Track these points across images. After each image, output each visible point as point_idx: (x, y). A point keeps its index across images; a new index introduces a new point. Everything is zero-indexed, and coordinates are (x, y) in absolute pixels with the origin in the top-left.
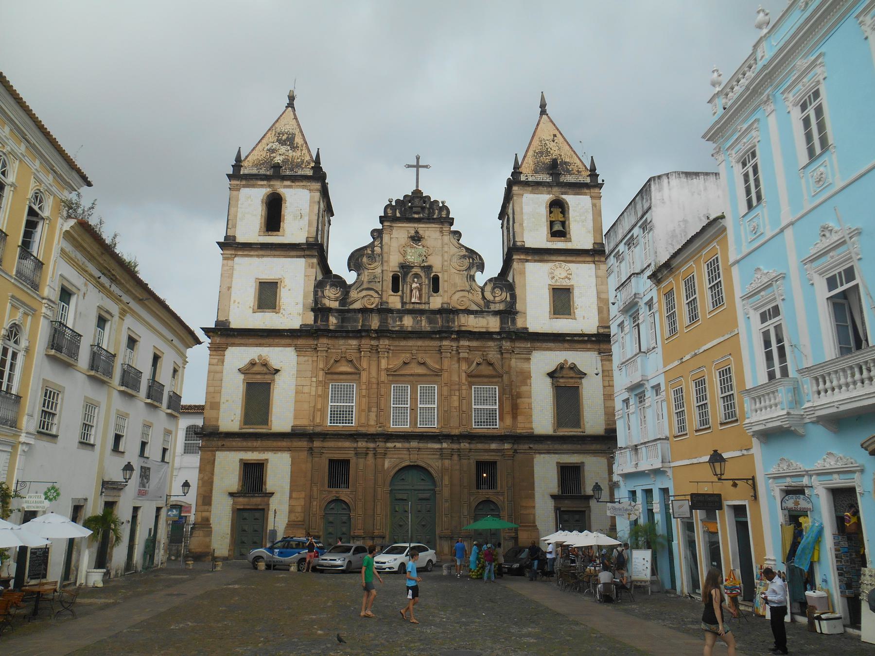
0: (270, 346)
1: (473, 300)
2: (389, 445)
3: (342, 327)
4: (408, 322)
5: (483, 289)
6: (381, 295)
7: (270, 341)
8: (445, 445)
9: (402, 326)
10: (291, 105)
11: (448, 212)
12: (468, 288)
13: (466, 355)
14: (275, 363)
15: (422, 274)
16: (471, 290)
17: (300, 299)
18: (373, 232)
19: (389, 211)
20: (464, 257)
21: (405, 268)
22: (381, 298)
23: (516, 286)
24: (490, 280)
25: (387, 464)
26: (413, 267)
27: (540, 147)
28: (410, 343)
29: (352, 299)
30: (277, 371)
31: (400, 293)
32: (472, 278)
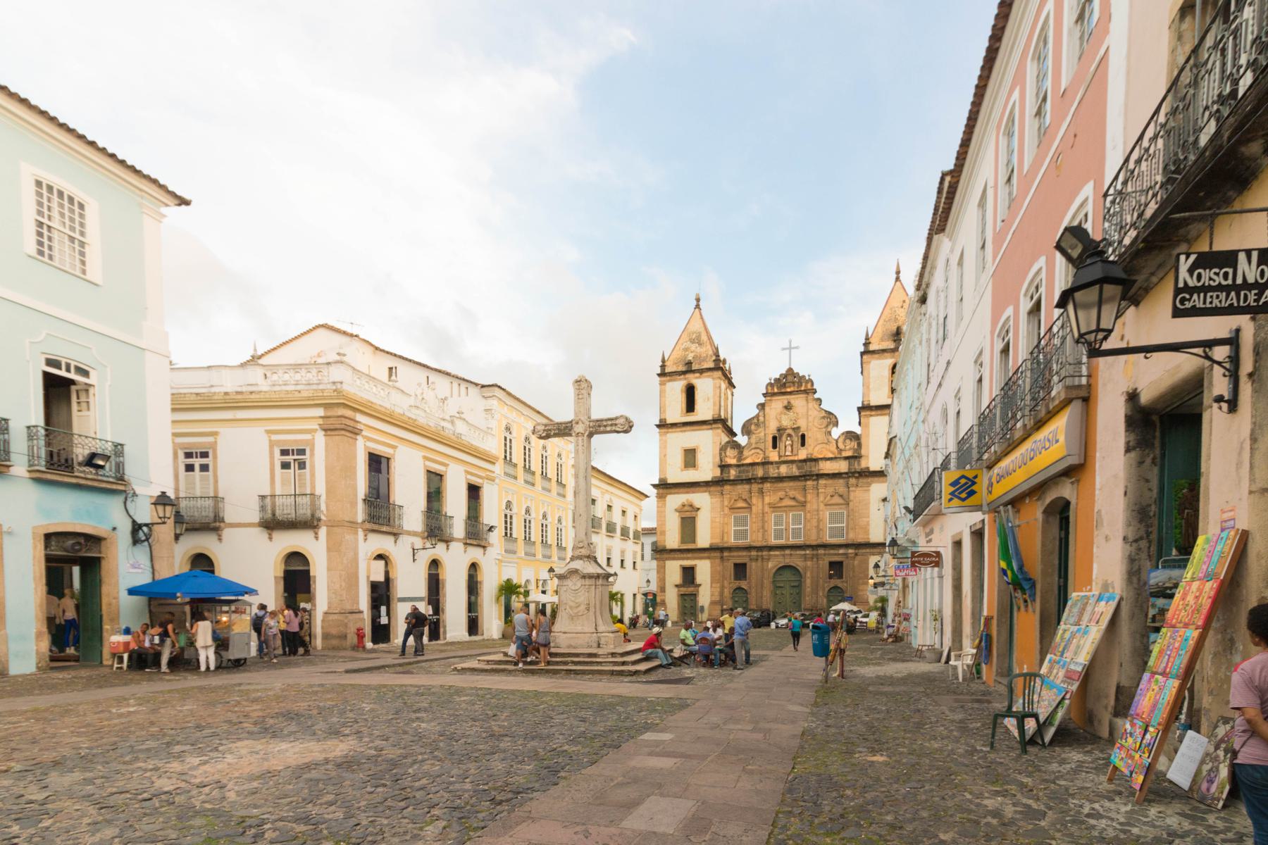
0: (693, 492)
1: (829, 451)
2: (772, 553)
3: (739, 476)
4: (784, 470)
7: (692, 489)
8: (808, 552)
9: (779, 473)
10: (698, 306)
11: (812, 385)
12: (826, 441)
13: (823, 490)
14: (697, 505)
15: (793, 434)
16: (828, 442)
17: (711, 459)
19: (769, 388)
20: (824, 417)
21: (781, 430)
24: (843, 434)
25: (770, 565)
28: (785, 484)
30: (699, 509)
32: (830, 433)
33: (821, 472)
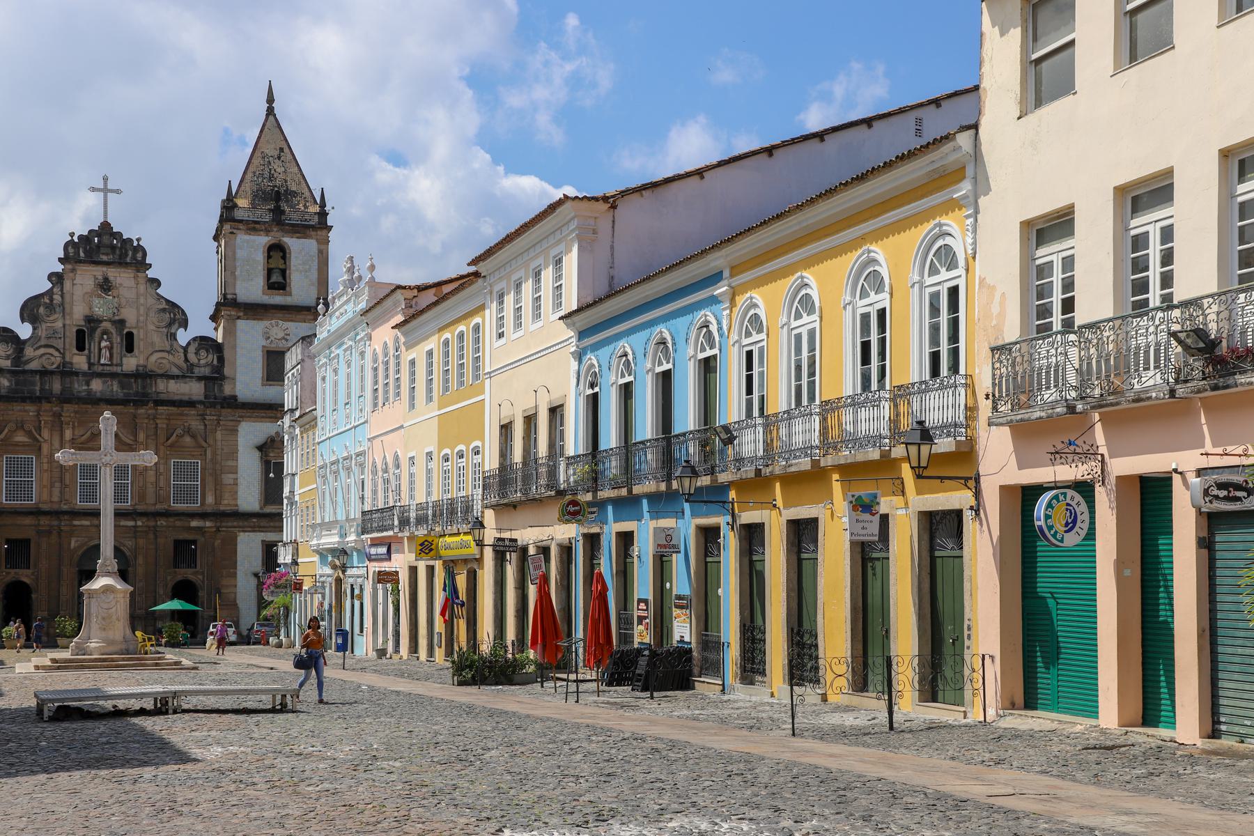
4: (97, 385)
5: (185, 349)
6: (63, 355)
8: (139, 523)
9: (89, 392)
18: (50, 277)
19: (71, 250)
20: (164, 310)
21: (92, 321)
22: (64, 358)
23: (225, 347)
24: (195, 339)
26: (101, 322)
27: (262, 167)
29: (25, 359)
31: (86, 352)
32: (173, 337)
33: (163, 397)
